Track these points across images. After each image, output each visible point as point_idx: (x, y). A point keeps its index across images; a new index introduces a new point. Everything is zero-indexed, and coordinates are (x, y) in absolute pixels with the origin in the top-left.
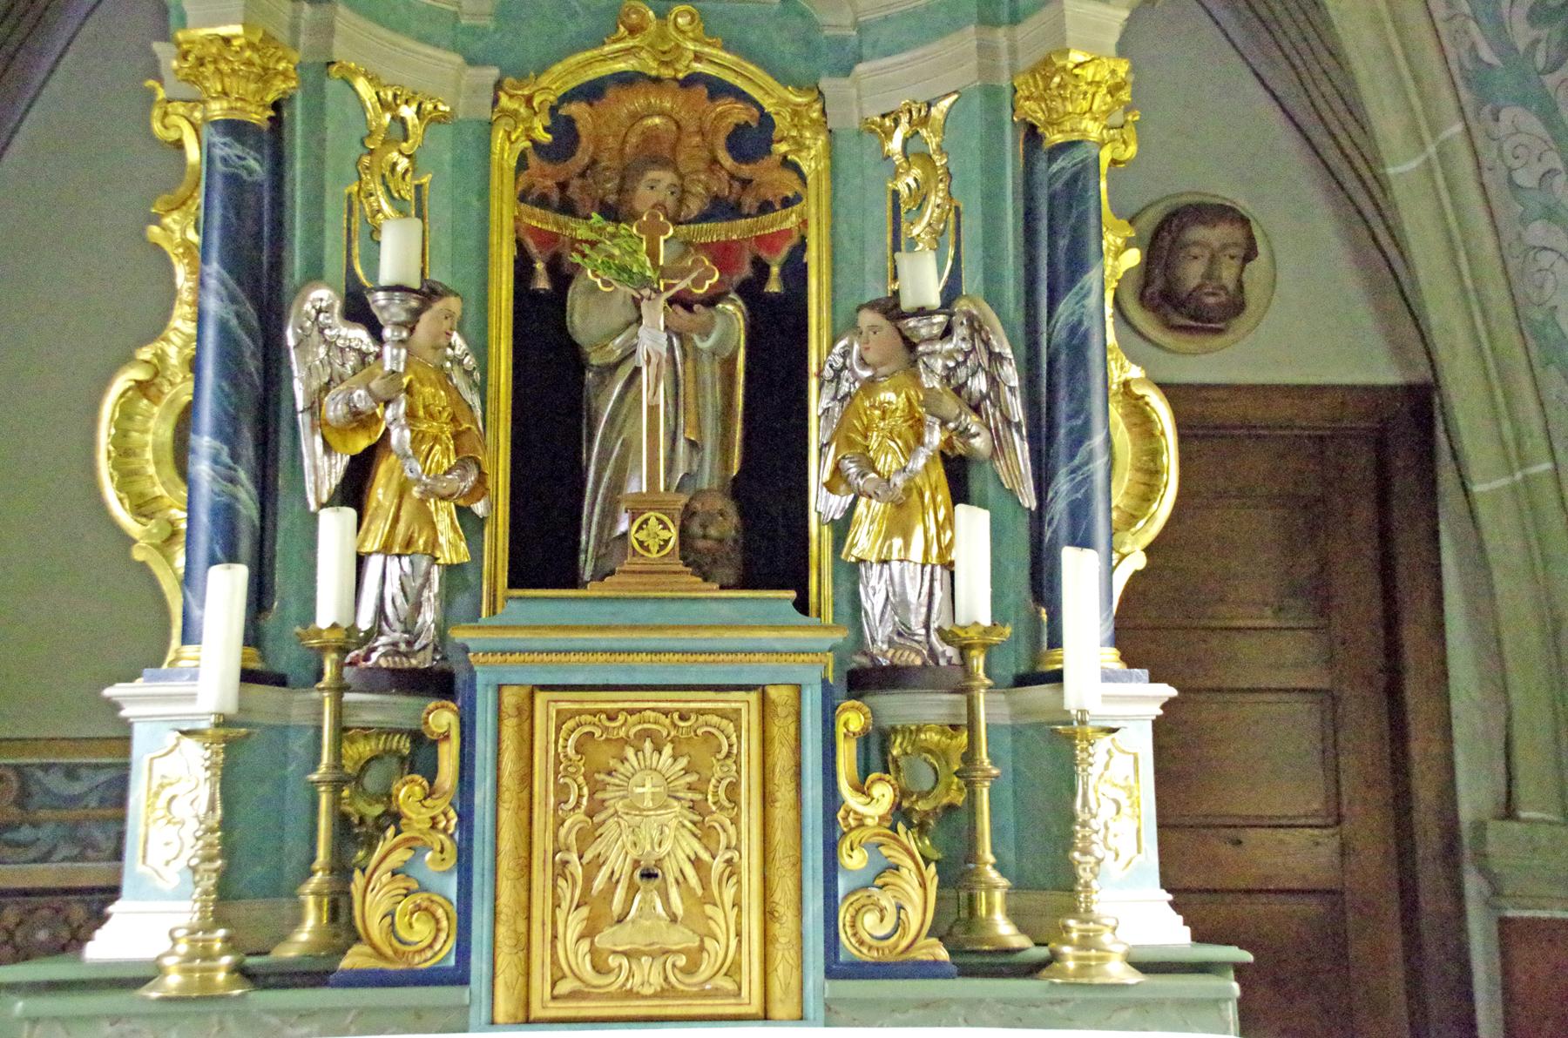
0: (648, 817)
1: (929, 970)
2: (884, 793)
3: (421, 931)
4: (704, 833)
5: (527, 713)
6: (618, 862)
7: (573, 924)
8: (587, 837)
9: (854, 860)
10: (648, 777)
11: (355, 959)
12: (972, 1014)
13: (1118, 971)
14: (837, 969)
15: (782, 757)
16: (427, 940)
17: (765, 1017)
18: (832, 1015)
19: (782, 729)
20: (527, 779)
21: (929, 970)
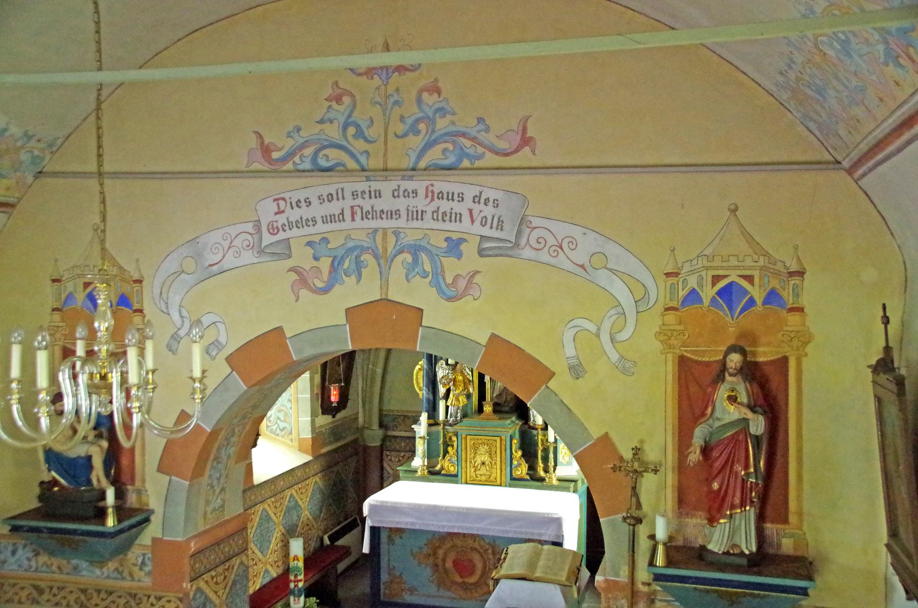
0: (482, 457)
1: (527, 480)
2: (520, 453)
3: (452, 469)
4: (491, 458)
5: (466, 439)
6: (479, 462)
7: (473, 470)
8: (474, 457)
9: (515, 463)
10: (483, 449)
11: (443, 472)
12: (531, 487)
13: (555, 482)
14: (512, 479)
15: (503, 447)
16: (453, 470)
17: (501, 485)
18: (510, 486)
19: (504, 442)
20: (466, 448)
21: (527, 480)
